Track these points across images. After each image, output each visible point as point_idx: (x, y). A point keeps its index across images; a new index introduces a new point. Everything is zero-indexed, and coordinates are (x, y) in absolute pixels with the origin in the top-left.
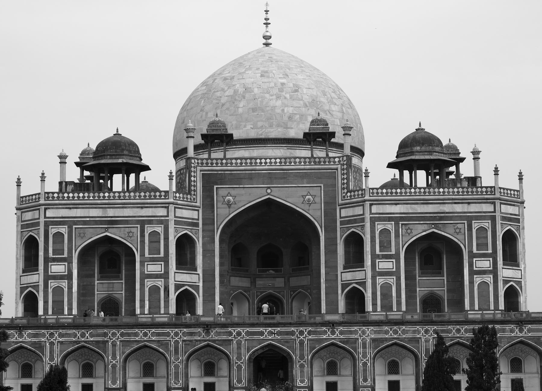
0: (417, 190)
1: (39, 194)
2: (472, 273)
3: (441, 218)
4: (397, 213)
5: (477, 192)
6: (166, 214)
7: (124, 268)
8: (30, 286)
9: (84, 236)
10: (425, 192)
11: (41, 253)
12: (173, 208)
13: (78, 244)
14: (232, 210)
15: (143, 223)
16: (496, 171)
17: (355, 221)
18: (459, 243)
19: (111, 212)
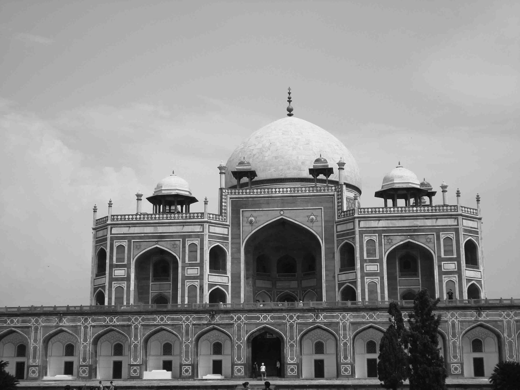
0: (396, 209)
1: (107, 217)
2: (441, 273)
3: (415, 231)
4: (380, 227)
5: (443, 210)
6: (201, 230)
7: (171, 272)
8: (100, 287)
9: (140, 248)
10: (402, 211)
11: (108, 261)
12: (208, 226)
13: (135, 254)
14: (254, 227)
15: (184, 237)
16: (458, 194)
17: (348, 234)
18: (430, 250)
19: (160, 229)
